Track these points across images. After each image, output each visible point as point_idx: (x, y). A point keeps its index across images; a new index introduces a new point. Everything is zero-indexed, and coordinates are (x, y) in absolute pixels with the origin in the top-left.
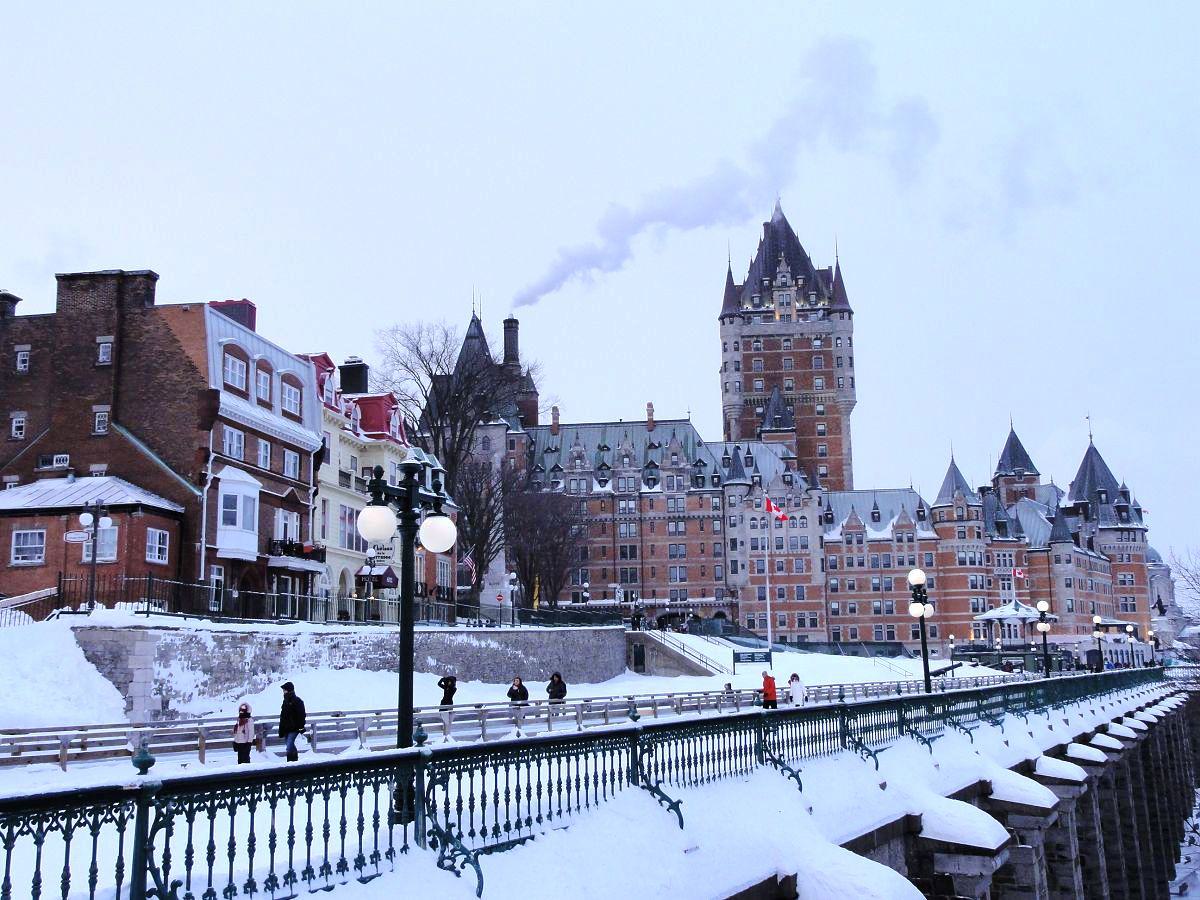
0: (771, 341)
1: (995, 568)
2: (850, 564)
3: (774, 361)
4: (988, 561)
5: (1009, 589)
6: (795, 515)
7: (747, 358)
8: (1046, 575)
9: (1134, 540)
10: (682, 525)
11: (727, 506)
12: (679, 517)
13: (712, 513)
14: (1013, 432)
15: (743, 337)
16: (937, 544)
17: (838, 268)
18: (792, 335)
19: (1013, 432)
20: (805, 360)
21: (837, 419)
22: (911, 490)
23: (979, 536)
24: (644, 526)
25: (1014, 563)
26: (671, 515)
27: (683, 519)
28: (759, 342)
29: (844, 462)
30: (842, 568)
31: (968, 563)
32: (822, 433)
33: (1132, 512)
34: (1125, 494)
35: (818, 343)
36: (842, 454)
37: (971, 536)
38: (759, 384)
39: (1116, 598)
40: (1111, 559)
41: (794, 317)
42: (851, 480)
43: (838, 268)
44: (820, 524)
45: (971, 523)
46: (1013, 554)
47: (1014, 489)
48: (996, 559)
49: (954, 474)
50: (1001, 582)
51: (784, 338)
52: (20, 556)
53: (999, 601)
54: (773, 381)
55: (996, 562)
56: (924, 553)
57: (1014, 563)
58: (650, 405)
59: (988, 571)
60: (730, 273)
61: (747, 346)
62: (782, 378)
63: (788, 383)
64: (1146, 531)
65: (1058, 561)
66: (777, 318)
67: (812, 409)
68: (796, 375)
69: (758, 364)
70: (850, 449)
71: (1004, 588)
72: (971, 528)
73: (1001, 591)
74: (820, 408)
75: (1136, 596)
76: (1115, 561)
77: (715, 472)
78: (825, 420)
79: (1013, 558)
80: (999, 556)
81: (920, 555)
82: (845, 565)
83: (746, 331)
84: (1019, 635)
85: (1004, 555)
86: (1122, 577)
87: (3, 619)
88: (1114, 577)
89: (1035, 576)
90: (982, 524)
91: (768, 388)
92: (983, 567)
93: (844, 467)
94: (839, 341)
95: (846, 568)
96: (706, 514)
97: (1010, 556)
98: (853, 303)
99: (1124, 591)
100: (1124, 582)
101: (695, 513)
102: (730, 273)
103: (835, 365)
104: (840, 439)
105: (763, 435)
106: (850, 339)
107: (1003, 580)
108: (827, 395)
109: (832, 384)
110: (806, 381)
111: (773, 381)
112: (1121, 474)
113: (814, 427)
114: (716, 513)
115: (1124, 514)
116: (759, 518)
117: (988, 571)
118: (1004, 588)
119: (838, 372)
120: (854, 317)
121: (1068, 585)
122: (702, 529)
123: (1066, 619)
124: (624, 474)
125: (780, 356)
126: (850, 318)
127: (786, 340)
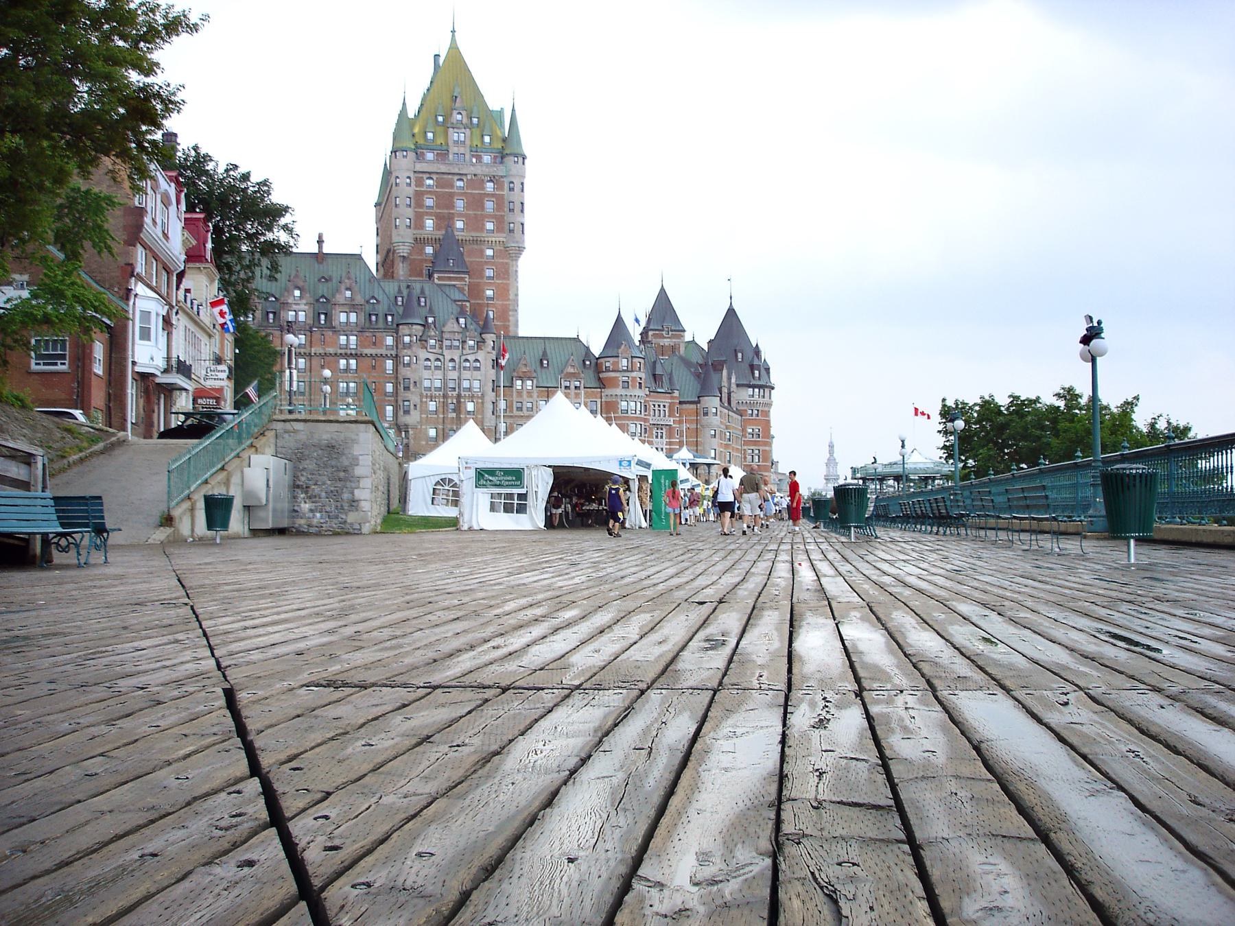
0: (444, 180)
2: (520, 409)
3: (446, 201)
4: (646, 411)
5: (662, 437)
6: (469, 357)
7: (419, 196)
9: (764, 397)
10: (353, 362)
11: (400, 346)
12: (351, 354)
13: (384, 352)
14: (663, 291)
15: (415, 172)
17: (513, 110)
18: (466, 175)
19: (663, 291)
20: (476, 202)
21: (507, 263)
22: (577, 340)
23: (640, 387)
24: (313, 362)
25: (667, 414)
26: (343, 351)
27: (352, 356)
28: (431, 178)
29: (511, 308)
30: (511, 411)
31: (629, 412)
32: (489, 278)
33: (762, 370)
34: (757, 352)
35: (490, 185)
36: (509, 299)
37: (634, 387)
38: (429, 223)
41: (467, 157)
42: (516, 325)
43: (513, 110)
44: (493, 368)
45: (634, 374)
46: (667, 405)
47: (661, 344)
49: (619, 323)
51: (456, 177)
52: (41, 362)
54: (445, 221)
55: (652, 413)
56: (589, 400)
57: (667, 414)
58: (320, 236)
59: (645, 420)
60: (404, 104)
61: (420, 182)
62: (453, 218)
63: (459, 225)
64: (773, 388)
65: (706, 414)
66: (451, 156)
67: (482, 252)
68: (466, 216)
69: (429, 202)
70: (517, 295)
71: (657, 437)
72: (634, 378)
74: (489, 252)
75: (761, 448)
77: (389, 309)
78: (493, 264)
79: (667, 409)
82: (515, 409)
83: (419, 167)
85: (659, 406)
86: (751, 430)
87: (156, 415)
90: (643, 376)
91: (437, 227)
92: (642, 416)
93: (511, 313)
94: (512, 185)
95: (516, 413)
96: (379, 351)
97: (664, 406)
98: (526, 149)
101: (368, 351)
102: (404, 104)
103: (506, 209)
104: (508, 285)
105: (436, 276)
106: (522, 184)
108: (497, 239)
109: (503, 228)
110: (475, 222)
111: (445, 221)
112: (755, 334)
113: (483, 270)
114: (389, 353)
115: (757, 373)
116: (432, 360)
117: (645, 420)
118: (657, 437)
119: (510, 217)
120: (526, 161)
122: (374, 367)
124: (295, 307)
125: (452, 195)
126: (523, 164)
127: (458, 180)
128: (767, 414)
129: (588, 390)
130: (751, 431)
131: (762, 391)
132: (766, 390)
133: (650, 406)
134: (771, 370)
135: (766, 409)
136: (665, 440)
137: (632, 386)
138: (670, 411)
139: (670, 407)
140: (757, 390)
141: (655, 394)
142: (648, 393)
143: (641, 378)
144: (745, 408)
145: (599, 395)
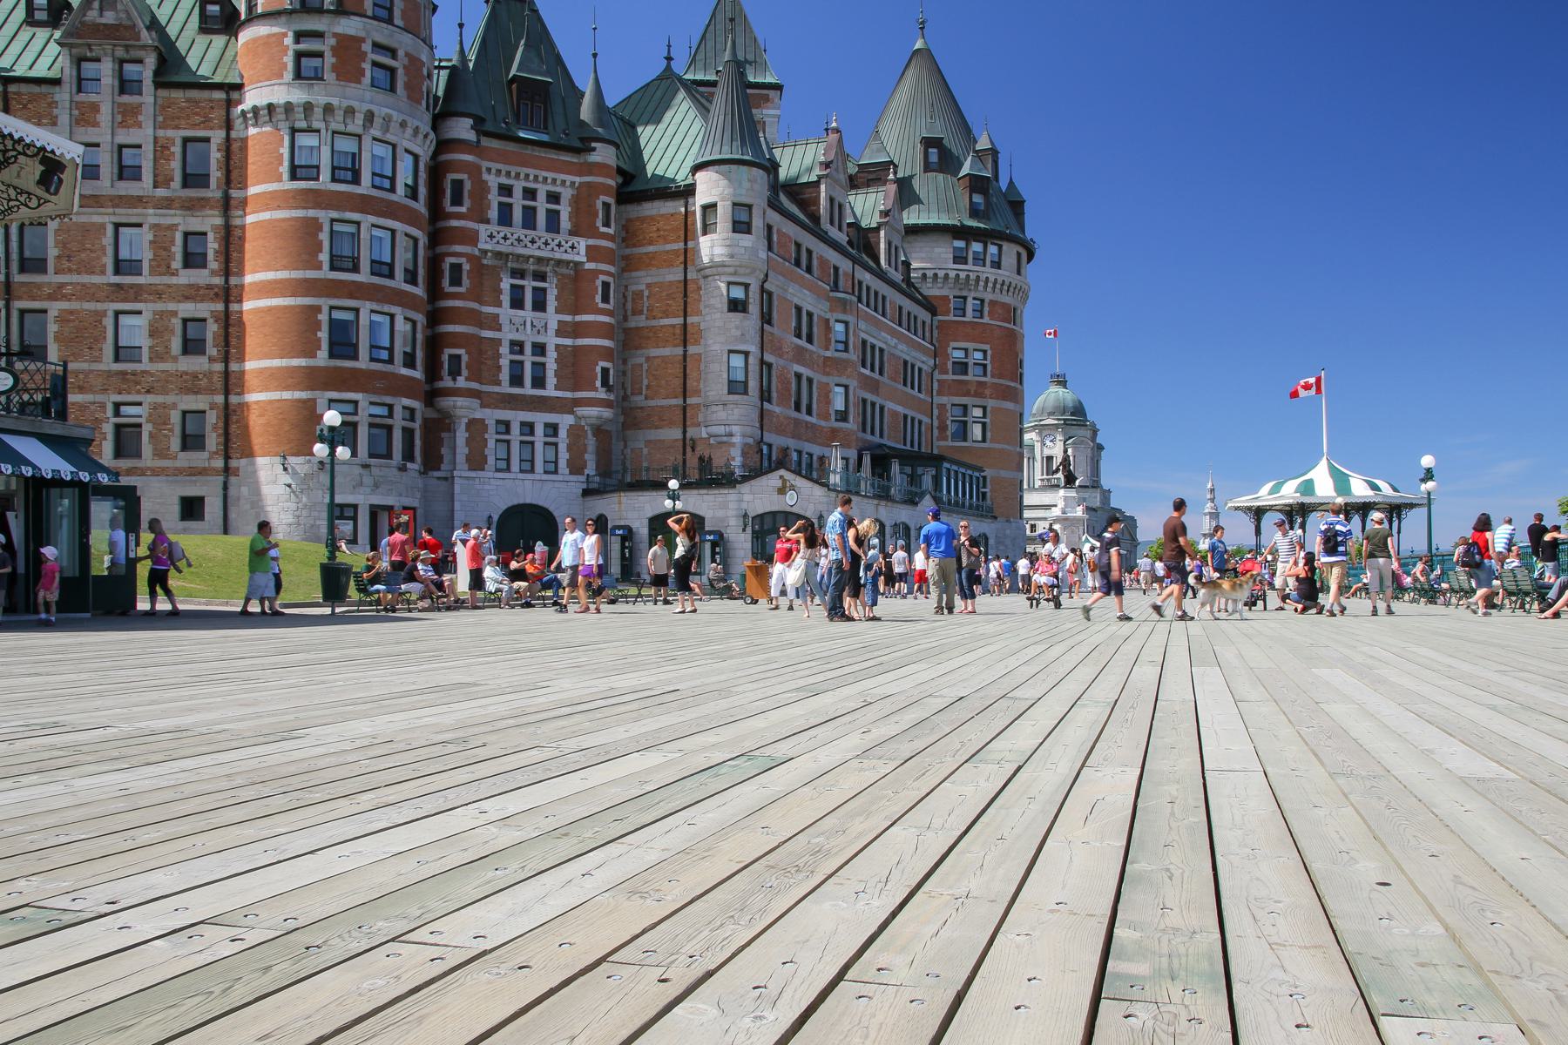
1: (484, 230)
5: (539, 305)
8: (675, 275)
9: (997, 265)
16: (230, 104)
39: (942, 407)
40: (930, 306)
46: (567, 194)
48: (494, 199)
50: (506, 284)
53: (498, 342)
55: (493, 213)
57: (565, 223)
72: (348, 48)
73: (505, 312)
76: (947, 313)
79: (565, 211)
80: (506, 190)
81: (161, 149)
84: (562, 463)
85: (530, 194)
88: (938, 353)
89: (643, 280)
97: (554, 198)
99: (961, 389)
100: (962, 367)
107: (520, 274)
118: (517, 303)
121: (736, 306)
123: (720, 414)
128: (1011, 314)
129: (177, 94)
130: (959, 354)
131: (993, 249)
132: (1006, 246)
133: (481, 189)
134: (1028, 208)
135: (1006, 299)
136: (552, 318)
137: (335, 68)
138: (575, 214)
139: (576, 202)
140: (977, 247)
141: (511, 147)
142: (471, 136)
143: (392, 52)
144: (945, 292)
145: (217, 115)
